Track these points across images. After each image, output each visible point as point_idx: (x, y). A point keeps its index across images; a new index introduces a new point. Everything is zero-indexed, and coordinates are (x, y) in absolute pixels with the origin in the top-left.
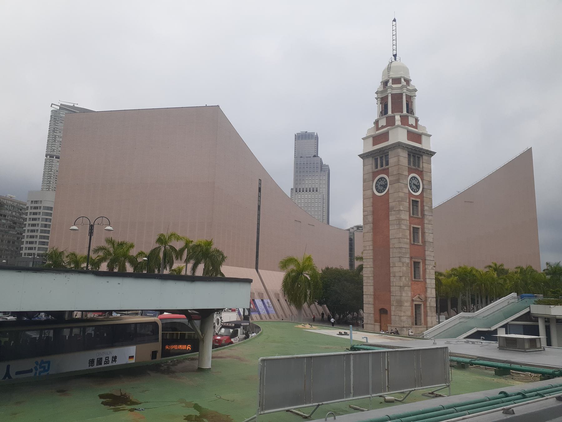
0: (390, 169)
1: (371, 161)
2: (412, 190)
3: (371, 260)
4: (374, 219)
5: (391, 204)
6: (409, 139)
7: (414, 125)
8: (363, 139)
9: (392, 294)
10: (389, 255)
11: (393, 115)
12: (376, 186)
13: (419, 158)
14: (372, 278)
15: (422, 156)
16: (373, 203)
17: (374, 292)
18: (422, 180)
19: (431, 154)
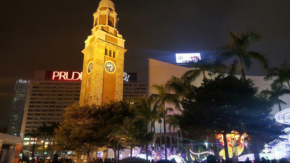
7: (113, 33)
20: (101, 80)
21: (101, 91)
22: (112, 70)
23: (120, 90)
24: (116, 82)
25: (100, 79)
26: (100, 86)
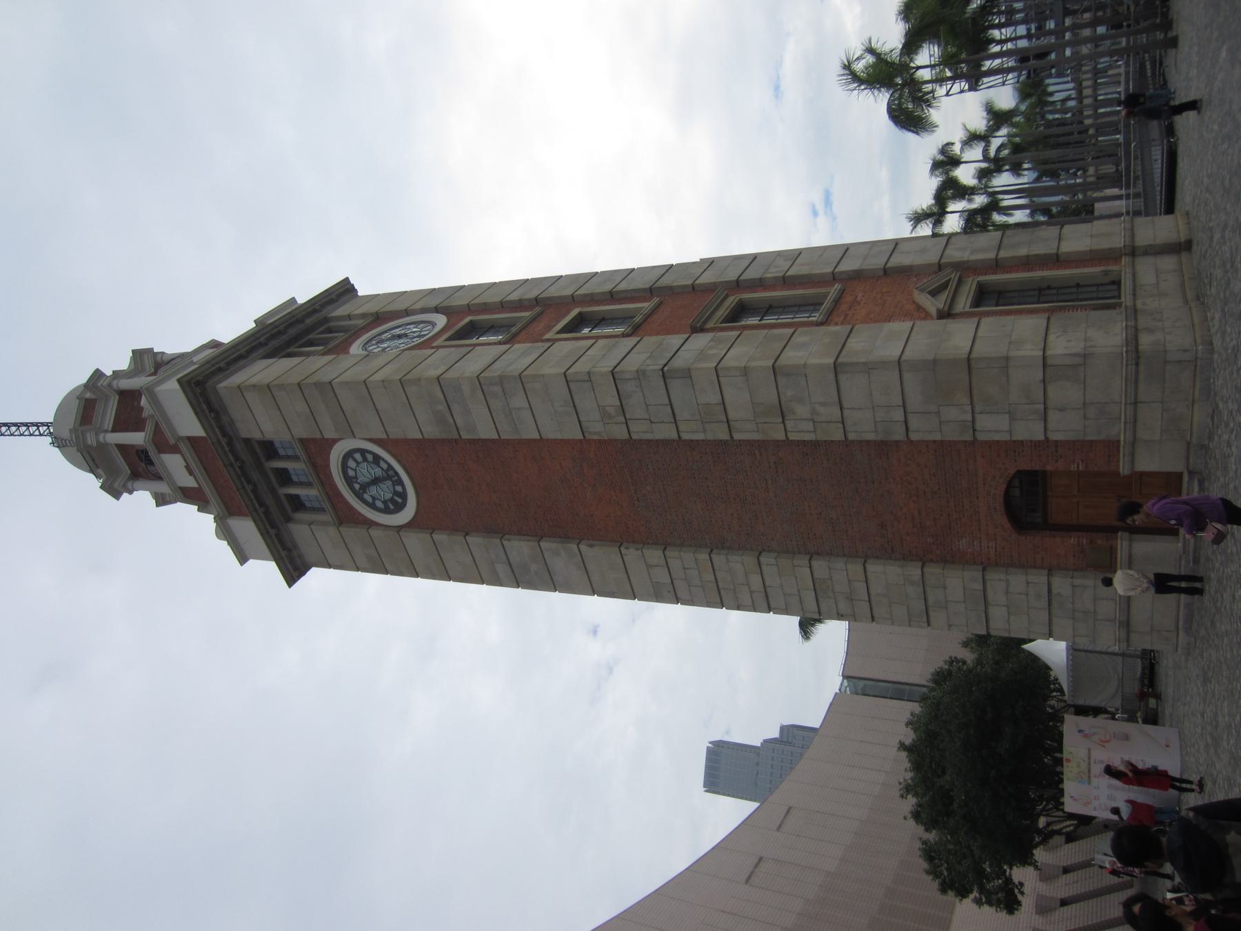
0: (300, 431)
1: (300, 531)
3: (719, 559)
4: (520, 533)
5: (431, 431)
8: (243, 559)
9: (899, 435)
10: (665, 442)
11: (149, 427)
12: (386, 511)
14: (820, 565)
15: (327, 320)
16: (453, 529)
17: (906, 557)
19: (344, 290)
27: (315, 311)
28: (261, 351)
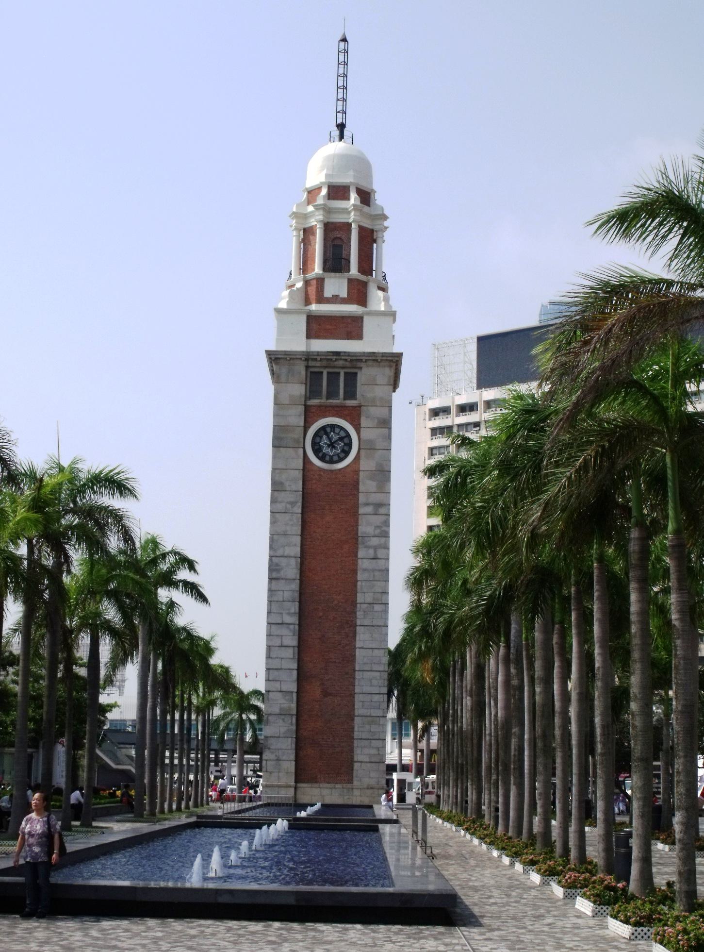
2: (322, 459)
6: (311, 334)
7: (344, 294)
13: (351, 378)
15: (361, 368)
18: (358, 428)
20: (293, 504)
21: (295, 545)
22: (342, 455)
23: (377, 527)
24: (362, 498)
25: (287, 503)
26: (288, 528)
27: (361, 360)
28: (311, 363)
